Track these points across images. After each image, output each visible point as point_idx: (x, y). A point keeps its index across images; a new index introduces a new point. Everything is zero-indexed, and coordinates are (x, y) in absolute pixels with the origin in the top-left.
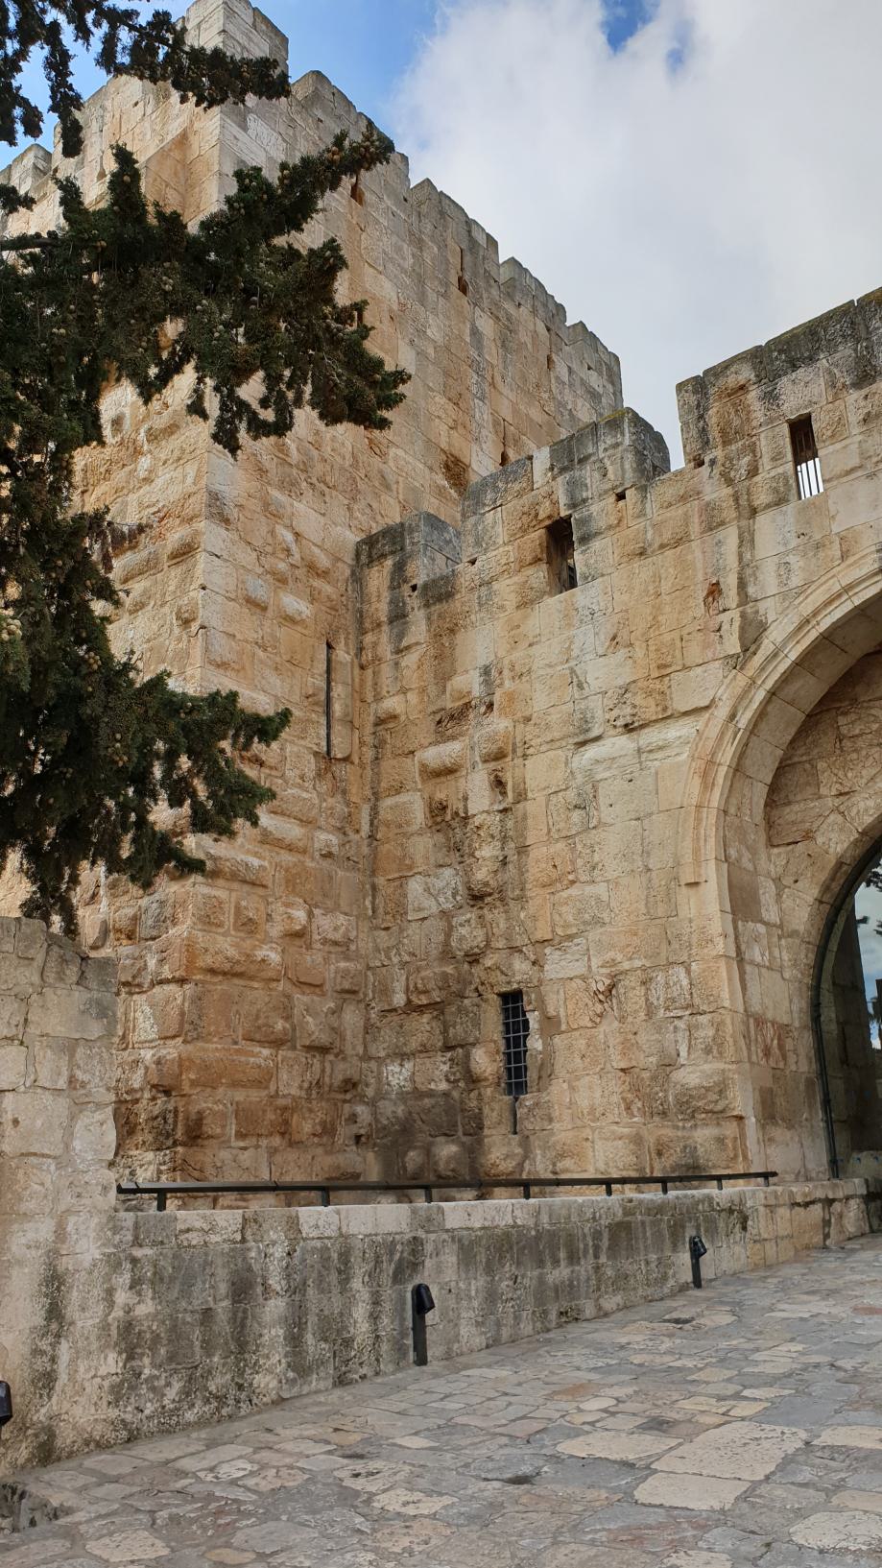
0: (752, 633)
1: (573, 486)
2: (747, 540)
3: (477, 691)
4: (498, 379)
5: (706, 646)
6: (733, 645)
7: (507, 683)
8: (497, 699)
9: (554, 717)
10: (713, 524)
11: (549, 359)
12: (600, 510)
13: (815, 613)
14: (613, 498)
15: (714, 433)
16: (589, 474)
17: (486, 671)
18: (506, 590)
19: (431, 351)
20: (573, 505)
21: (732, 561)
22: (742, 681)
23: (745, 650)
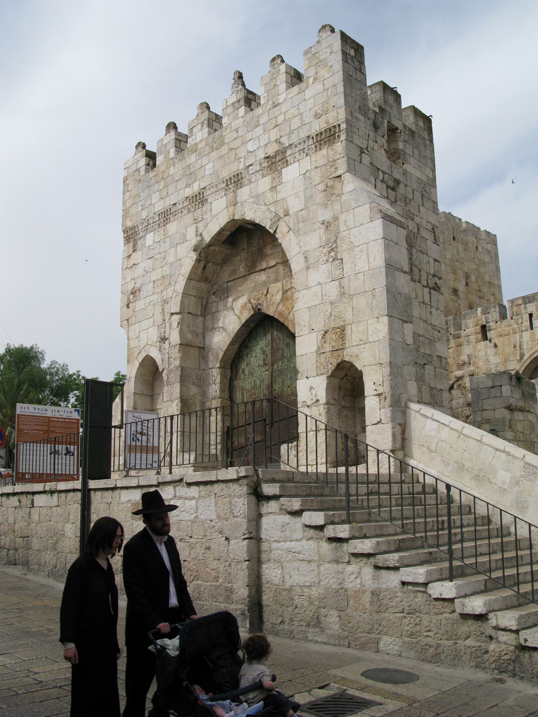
0: (522, 356)
1: (486, 318)
2: (521, 337)
3: (467, 360)
4: (464, 261)
5: (514, 357)
6: (518, 358)
7: (474, 359)
8: (471, 362)
9: (484, 368)
10: (515, 333)
11: (477, 247)
12: (492, 325)
13: (533, 354)
14: (494, 323)
15: (515, 313)
16: (489, 316)
17: (469, 356)
18: (472, 338)
19: (448, 262)
20: (487, 322)
21: (518, 341)
22: (520, 365)
23: (521, 359)
